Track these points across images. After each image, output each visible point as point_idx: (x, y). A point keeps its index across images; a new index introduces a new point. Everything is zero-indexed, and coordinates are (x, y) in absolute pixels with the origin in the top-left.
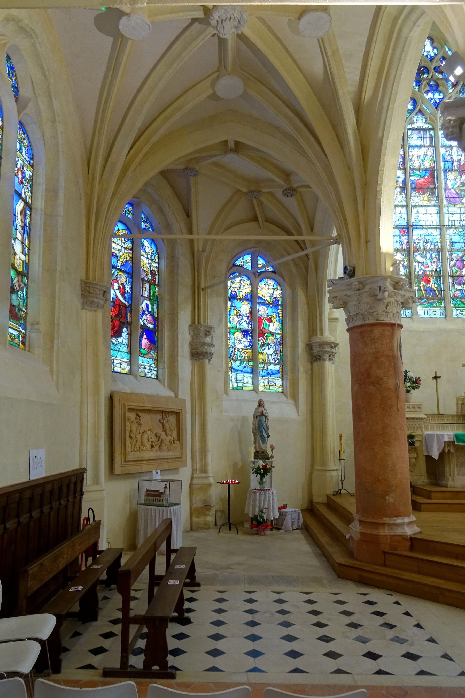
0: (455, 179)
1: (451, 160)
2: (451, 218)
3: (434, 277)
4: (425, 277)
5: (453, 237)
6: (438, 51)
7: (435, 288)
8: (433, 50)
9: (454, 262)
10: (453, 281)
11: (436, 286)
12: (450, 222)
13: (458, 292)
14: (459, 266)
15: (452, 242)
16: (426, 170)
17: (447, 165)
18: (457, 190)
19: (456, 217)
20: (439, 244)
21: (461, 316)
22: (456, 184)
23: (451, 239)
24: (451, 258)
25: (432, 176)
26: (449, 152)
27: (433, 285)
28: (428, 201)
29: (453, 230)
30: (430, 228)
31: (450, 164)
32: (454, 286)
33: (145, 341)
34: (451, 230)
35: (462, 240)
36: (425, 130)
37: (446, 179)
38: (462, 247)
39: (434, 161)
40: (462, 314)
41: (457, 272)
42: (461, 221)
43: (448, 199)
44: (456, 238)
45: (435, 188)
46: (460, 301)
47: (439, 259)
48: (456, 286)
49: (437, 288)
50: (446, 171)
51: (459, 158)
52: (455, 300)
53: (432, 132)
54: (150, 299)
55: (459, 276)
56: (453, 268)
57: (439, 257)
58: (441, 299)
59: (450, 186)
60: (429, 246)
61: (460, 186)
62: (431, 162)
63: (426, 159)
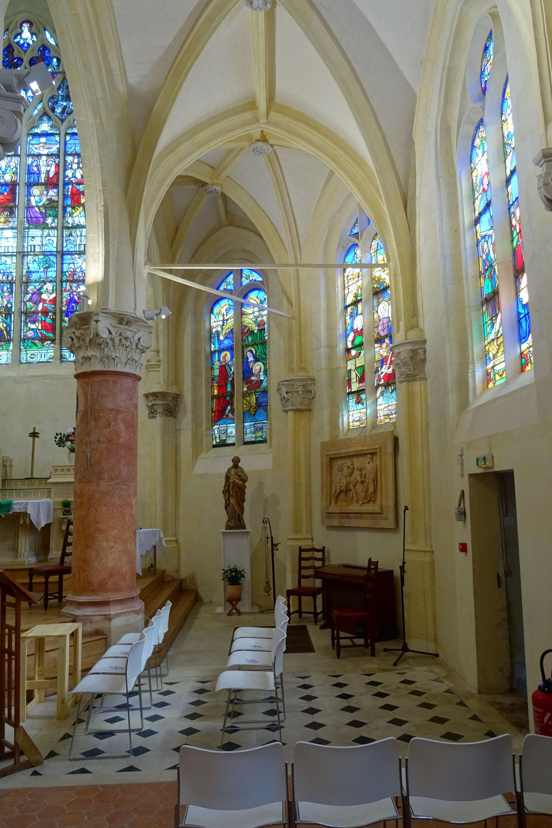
0: (41, 195)
1: (38, 172)
2: (31, 243)
3: (4, 315)
5: (30, 265)
6: (37, 38)
7: (3, 328)
8: (32, 37)
9: (30, 295)
10: (26, 319)
11: (5, 325)
12: (29, 247)
13: (31, 332)
14: (35, 300)
15: (29, 272)
16: (6, 184)
17: (32, 178)
18: (42, 209)
19: (37, 241)
20: (14, 274)
21: (31, 360)
22: (41, 201)
23: (29, 268)
24: (27, 290)
25: (13, 192)
26: (36, 162)
28: (4, 223)
29: (32, 257)
30: (4, 255)
31: (36, 176)
32: (27, 325)
34: (30, 257)
35: (42, 269)
37: (29, 194)
38: (40, 277)
39: (17, 173)
40: (33, 358)
41: (31, 308)
42: (42, 245)
43: (30, 219)
44: (34, 267)
45: (15, 206)
46: (32, 342)
47: (11, 293)
48: (29, 325)
49: (6, 328)
50: (30, 185)
51: (48, 169)
52: (27, 341)
55: (34, 313)
56: (28, 303)
57: (12, 292)
58: (9, 341)
59: (34, 204)
61: (47, 203)
62: (13, 175)
63: (8, 171)
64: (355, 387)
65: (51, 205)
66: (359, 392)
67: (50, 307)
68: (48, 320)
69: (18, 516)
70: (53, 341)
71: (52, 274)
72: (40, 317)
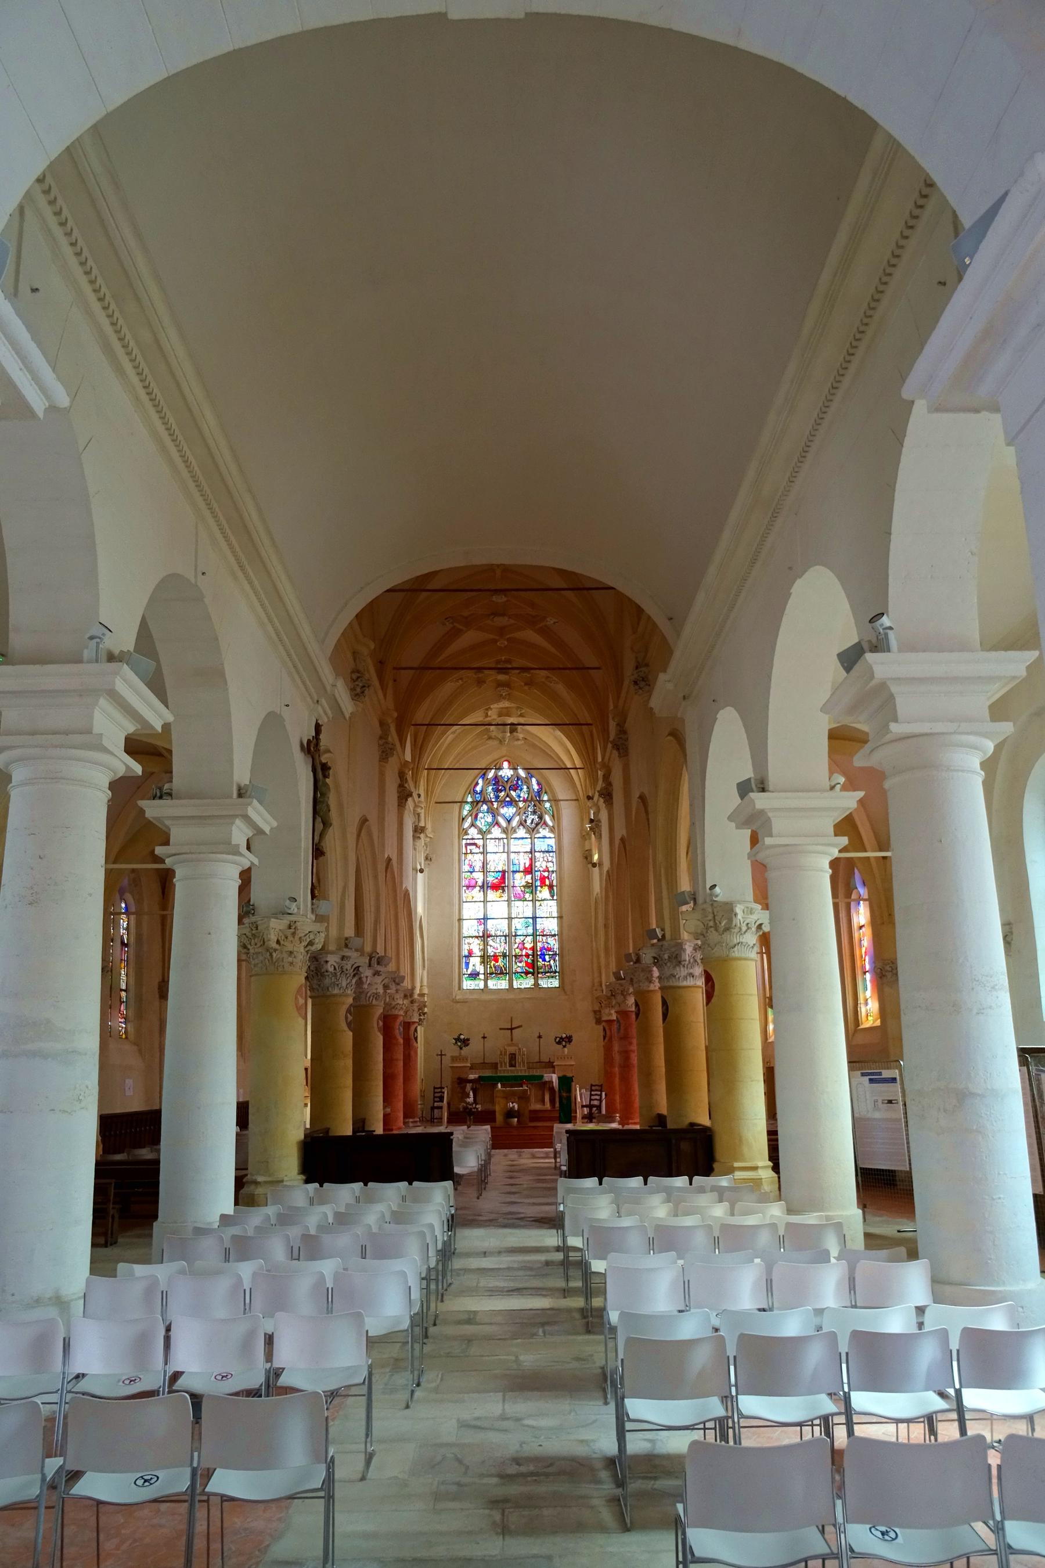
4: (495, 958)
19: (520, 910)
25: (503, 877)
27: (500, 963)
50: (514, 872)
59: (516, 884)
65: (528, 886)
67: (530, 952)
69: (546, 1082)
70: (533, 974)
71: (530, 931)
72: (525, 959)
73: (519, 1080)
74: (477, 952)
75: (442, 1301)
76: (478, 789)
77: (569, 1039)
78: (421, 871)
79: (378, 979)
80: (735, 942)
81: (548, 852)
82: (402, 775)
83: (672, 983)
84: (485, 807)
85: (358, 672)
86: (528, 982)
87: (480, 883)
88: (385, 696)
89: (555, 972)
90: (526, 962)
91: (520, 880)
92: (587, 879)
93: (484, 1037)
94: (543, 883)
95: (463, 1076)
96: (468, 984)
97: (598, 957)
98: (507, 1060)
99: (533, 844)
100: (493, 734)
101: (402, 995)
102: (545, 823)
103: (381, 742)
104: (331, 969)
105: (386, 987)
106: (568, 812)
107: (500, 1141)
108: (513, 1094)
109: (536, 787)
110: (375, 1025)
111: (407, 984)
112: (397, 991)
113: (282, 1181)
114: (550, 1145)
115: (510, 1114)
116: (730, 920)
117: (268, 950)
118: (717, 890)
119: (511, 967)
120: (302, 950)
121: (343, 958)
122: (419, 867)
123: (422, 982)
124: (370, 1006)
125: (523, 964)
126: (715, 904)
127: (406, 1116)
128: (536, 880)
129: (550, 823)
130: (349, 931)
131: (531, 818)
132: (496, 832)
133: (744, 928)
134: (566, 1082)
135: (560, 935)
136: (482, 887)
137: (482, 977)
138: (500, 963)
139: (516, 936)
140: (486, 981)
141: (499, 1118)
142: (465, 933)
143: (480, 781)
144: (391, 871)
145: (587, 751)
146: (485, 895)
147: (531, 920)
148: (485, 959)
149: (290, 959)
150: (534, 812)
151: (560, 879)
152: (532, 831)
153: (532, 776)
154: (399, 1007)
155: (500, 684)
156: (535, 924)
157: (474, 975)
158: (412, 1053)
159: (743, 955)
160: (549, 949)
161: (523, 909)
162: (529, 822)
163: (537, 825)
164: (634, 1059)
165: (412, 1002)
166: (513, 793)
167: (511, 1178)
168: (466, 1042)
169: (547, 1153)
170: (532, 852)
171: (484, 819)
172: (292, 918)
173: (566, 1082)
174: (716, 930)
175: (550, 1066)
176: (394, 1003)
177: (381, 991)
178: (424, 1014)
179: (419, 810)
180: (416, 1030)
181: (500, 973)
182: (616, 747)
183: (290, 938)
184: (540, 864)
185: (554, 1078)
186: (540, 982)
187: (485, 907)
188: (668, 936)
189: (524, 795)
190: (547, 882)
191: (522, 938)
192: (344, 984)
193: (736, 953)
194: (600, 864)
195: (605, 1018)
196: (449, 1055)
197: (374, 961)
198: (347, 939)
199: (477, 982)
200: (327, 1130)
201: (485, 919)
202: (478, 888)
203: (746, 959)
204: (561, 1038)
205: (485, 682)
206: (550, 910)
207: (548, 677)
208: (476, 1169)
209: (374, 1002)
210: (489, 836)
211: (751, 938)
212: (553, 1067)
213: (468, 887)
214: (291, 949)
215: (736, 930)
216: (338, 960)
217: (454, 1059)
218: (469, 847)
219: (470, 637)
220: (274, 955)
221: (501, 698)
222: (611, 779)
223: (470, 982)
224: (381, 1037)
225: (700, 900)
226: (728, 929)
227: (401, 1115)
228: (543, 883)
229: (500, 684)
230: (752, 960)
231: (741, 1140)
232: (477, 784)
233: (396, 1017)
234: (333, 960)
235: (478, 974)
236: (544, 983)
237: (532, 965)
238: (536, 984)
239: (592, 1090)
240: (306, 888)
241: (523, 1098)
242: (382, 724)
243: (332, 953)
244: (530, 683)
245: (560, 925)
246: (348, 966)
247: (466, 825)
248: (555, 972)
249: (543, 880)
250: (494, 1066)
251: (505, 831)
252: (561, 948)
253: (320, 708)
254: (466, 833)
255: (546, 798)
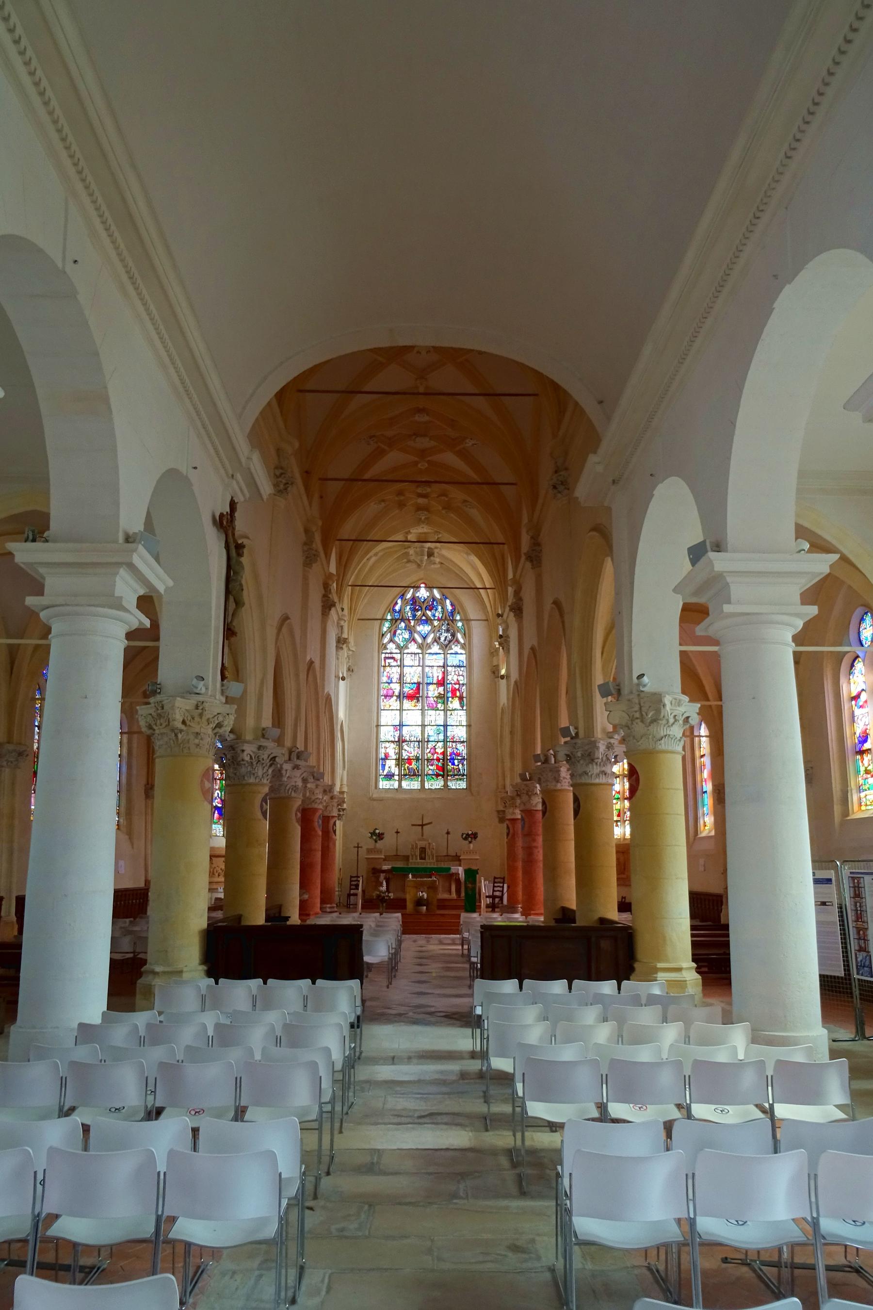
4: (409, 760)
19: (433, 718)
25: (418, 688)
27: (414, 765)
33: (216, 815)
36: (415, 654)
50: (428, 684)
53: (421, 656)
54: (220, 789)
59: (430, 695)
60: (413, 739)
64: (615, 818)
66: (617, 821)
67: (441, 757)
68: (440, 764)
71: (441, 737)
72: (436, 762)
73: (429, 872)
74: (393, 756)
75: (341, 1132)
76: (397, 608)
77: (475, 836)
78: (343, 679)
79: (297, 773)
80: (662, 734)
81: (459, 666)
82: (326, 586)
83: (585, 780)
84: (403, 625)
85: (282, 468)
86: (438, 784)
87: (397, 693)
88: (310, 504)
89: (463, 775)
90: (437, 765)
91: (433, 691)
92: (493, 692)
93: (397, 832)
94: (454, 695)
95: (378, 867)
96: (384, 784)
97: (503, 762)
98: (418, 853)
99: (445, 659)
100: (412, 558)
101: (322, 790)
102: (458, 641)
103: (305, 548)
104: (247, 758)
105: (305, 781)
106: (478, 631)
107: (408, 928)
108: (422, 884)
109: (449, 608)
110: (294, 817)
111: (327, 780)
112: (317, 786)
113: (181, 972)
114: (457, 932)
115: (419, 902)
116: (658, 711)
117: (173, 730)
118: (645, 679)
119: (423, 770)
120: (210, 732)
121: (260, 748)
122: (341, 675)
123: (342, 780)
124: (289, 798)
125: (434, 767)
126: (642, 695)
127: (323, 902)
128: (448, 693)
129: (462, 641)
130: (267, 722)
131: (444, 636)
132: (413, 648)
133: (671, 720)
134: (471, 874)
135: (468, 742)
136: (399, 697)
137: (396, 778)
138: (414, 765)
139: (428, 741)
140: (400, 781)
141: (410, 906)
142: (382, 738)
143: (399, 601)
144: (314, 673)
145: (497, 570)
146: (401, 704)
147: (442, 728)
148: (399, 761)
149: (197, 741)
150: (448, 631)
151: (469, 691)
152: (445, 647)
153: (446, 598)
154: (318, 801)
155: (419, 508)
156: (445, 731)
157: (390, 776)
158: (331, 845)
159: (670, 748)
160: (458, 755)
161: (435, 717)
162: (442, 639)
163: (450, 642)
164: (539, 855)
165: (332, 798)
166: (429, 613)
167: (421, 965)
168: (380, 836)
169: (453, 939)
170: (445, 666)
171: (402, 635)
172: (200, 698)
173: (471, 874)
174: (642, 721)
175: (457, 859)
176: (313, 798)
177: (300, 784)
178: (343, 810)
179: (342, 623)
180: (335, 824)
181: (413, 774)
182: (529, 558)
183: (197, 719)
184: (452, 678)
185: (461, 870)
186: (449, 784)
187: (401, 715)
188: (581, 734)
189: (438, 614)
190: (458, 694)
191: (434, 744)
192: (260, 773)
193: (663, 745)
194: (506, 677)
195: (509, 817)
196: (365, 848)
197: (294, 756)
198: (264, 729)
199: (392, 782)
200: (239, 918)
201: (401, 725)
202: (395, 698)
203: (672, 752)
204: (468, 834)
205: (405, 505)
206: (459, 719)
207: (465, 501)
208: (386, 959)
209: (293, 794)
210: (406, 651)
211: (677, 731)
212: (460, 860)
213: (386, 696)
214: (198, 731)
215: (664, 722)
216: (255, 750)
217: (369, 851)
218: (387, 661)
219: (393, 458)
220: (180, 736)
221: (419, 522)
222: (522, 594)
223: (385, 782)
224: (299, 828)
225: (625, 691)
226: (655, 720)
227: (318, 901)
228: (454, 695)
229: (419, 508)
230: (678, 753)
231: (664, 939)
232: (396, 603)
233: (315, 810)
234: (249, 750)
235: (393, 775)
236: (453, 785)
237: (442, 769)
238: (446, 785)
239: (495, 882)
240: (215, 668)
241: (432, 888)
242: (307, 531)
243: (248, 742)
244: (448, 507)
245: (469, 733)
246: (265, 755)
247: (386, 640)
248: (463, 775)
249: (454, 691)
250: (406, 858)
251: (420, 646)
252: (469, 753)
253: (234, 482)
254: (385, 648)
255: (458, 618)
